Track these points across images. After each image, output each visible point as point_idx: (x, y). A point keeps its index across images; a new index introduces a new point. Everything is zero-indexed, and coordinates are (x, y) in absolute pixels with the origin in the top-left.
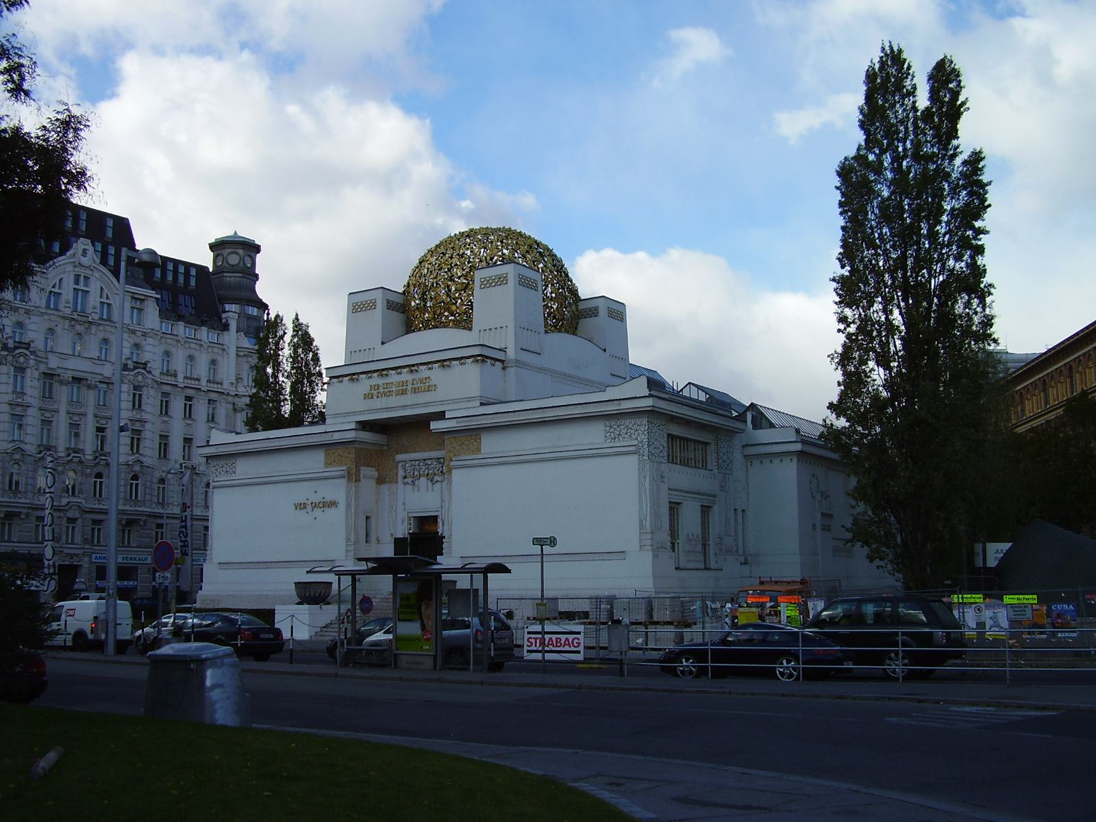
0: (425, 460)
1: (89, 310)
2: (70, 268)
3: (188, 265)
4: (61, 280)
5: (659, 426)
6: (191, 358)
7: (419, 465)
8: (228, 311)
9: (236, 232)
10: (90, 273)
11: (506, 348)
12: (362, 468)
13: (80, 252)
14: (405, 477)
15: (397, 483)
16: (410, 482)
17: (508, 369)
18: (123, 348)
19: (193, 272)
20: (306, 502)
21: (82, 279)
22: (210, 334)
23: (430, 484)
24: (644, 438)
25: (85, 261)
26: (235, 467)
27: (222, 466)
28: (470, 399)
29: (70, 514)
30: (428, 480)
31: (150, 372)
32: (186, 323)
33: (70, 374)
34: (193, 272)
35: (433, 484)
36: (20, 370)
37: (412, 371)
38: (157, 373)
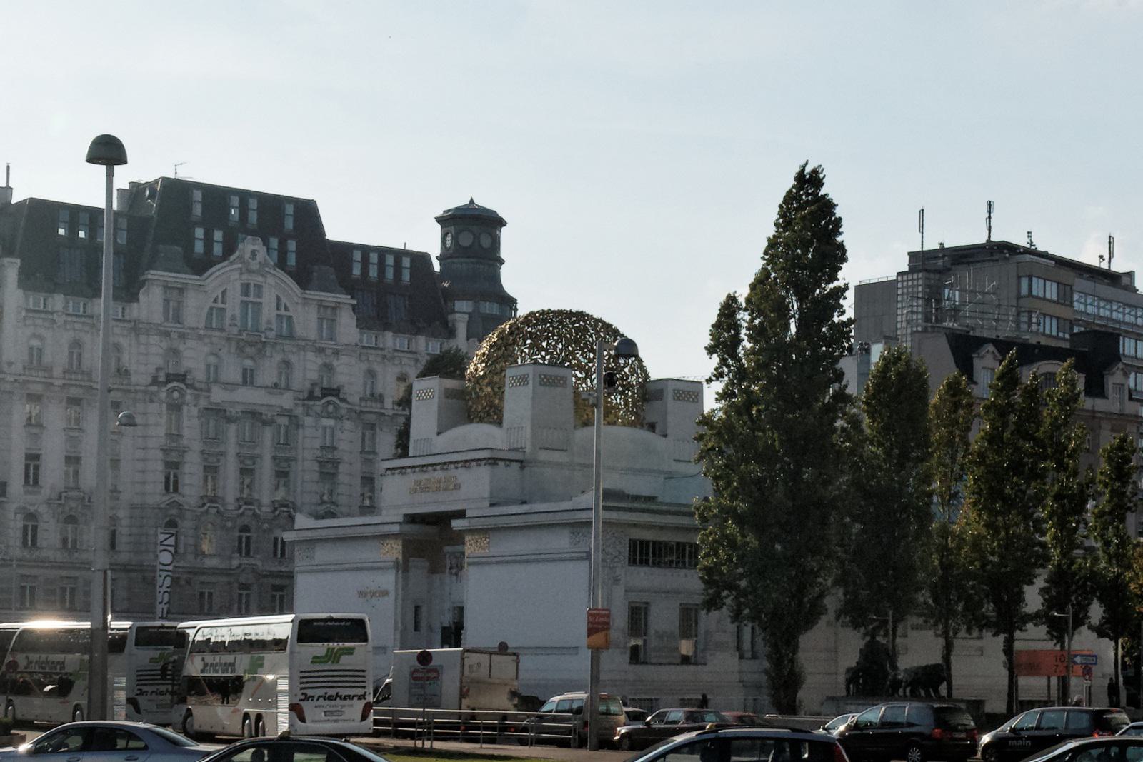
1: (264, 326)
2: (235, 275)
4: (224, 292)
10: (261, 279)
13: (248, 255)
14: (451, 568)
18: (308, 369)
19: (406, 262)
21: (252, 288)
22: (430, 344)
25: (254, 265)
29: (242, 580)
31: (344, 400)
33: (239, 408)
36: (175, 408)
37: (443, 469)
38: (354, 399)
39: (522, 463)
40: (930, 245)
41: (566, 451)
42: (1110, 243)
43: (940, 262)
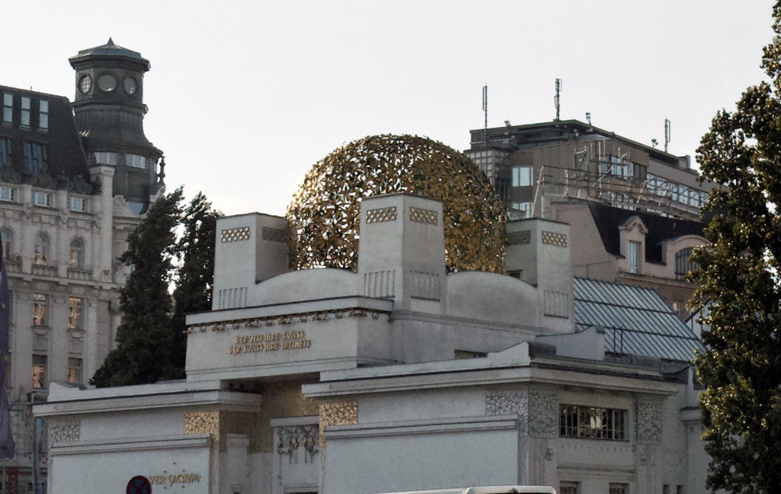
0: (303, 426)
3: (36, 98)
5: (545, 398)
6: (44, 236)
7: (296, 432)
8: (99, 165)
9: (111, 42)
11: (393, 297)
12: (229, 435)
14: (281, 446)
15: (272, 451)
16: (286, 451)
17: (397, 322)
19: (44, 106)
20: (165, 475)
22: (72, 199)
23: (308, 454)
24: (524, 411)
26: (79, 430)
27: (63, 429)
28: (349, 358)
30: (306, 450)
32: (35, 186)
34: (44, 106)
35: (312, 455)
37: (284, 323)
39: (391, 315)
40: (496, 123)
41: (439, 300)
42: (666, 126)
43: (506, 141)
